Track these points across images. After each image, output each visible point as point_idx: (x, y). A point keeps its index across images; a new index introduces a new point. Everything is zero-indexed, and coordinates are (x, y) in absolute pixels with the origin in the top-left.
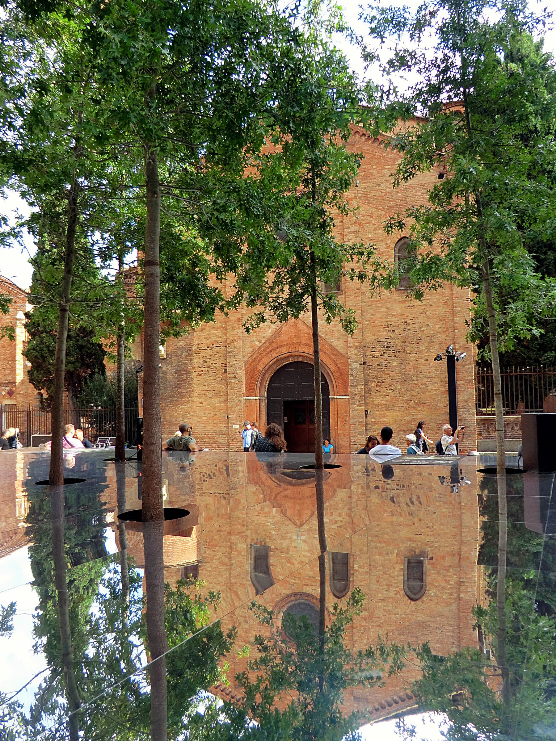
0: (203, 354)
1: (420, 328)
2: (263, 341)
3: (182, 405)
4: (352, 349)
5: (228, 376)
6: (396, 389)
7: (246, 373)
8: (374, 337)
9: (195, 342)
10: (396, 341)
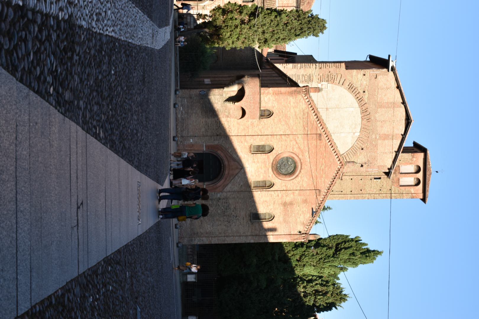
1: (234, 222)
2: (231, 153)
3: (201, 113)
4: (226, 194)
5: (215, 137)
7: (216, 145)
8: (231, 203)
9: (232, 120)
10: (229, 212)
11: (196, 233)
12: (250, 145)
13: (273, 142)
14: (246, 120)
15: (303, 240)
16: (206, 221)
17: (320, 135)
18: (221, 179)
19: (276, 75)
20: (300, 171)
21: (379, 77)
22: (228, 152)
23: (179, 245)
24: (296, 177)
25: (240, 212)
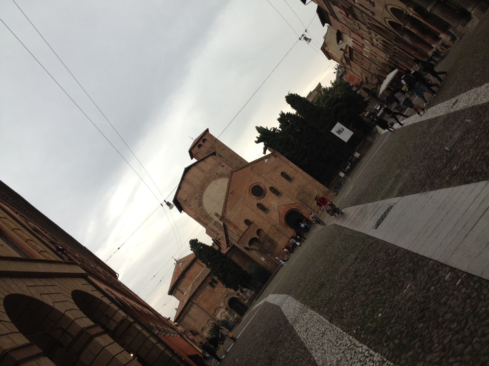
0: (270, 232)
6: (310, 199)
9: (266, 232)
11: (323, 194)
12: (267, 214)
13: (255, 207)
14: (260, 227)
15: (277, 152)
16: (314, 194)
17: (231, 193)
18: (291, 209)
19: (229, 237)
20: (253, 184)
21: (184, 199)
22: (279, 219)
23: (336, 194)
24: (258, 183)
25: (295, 187)
